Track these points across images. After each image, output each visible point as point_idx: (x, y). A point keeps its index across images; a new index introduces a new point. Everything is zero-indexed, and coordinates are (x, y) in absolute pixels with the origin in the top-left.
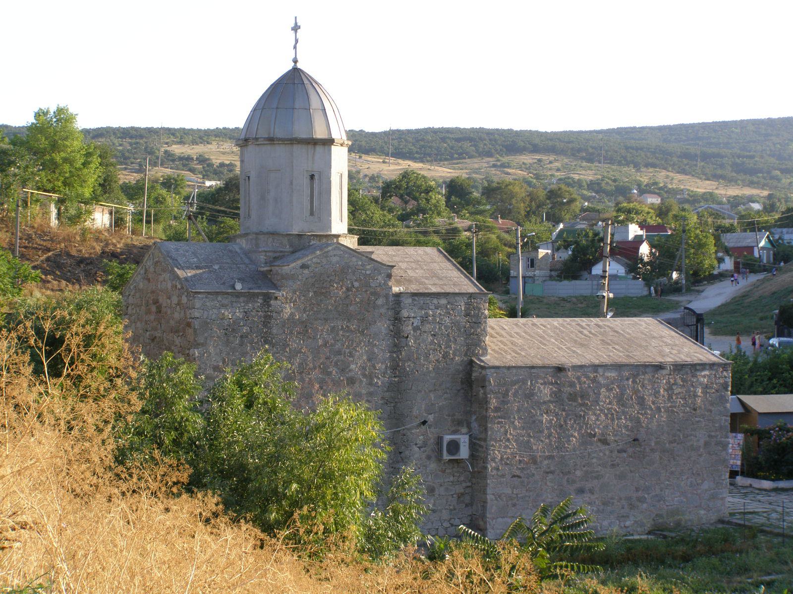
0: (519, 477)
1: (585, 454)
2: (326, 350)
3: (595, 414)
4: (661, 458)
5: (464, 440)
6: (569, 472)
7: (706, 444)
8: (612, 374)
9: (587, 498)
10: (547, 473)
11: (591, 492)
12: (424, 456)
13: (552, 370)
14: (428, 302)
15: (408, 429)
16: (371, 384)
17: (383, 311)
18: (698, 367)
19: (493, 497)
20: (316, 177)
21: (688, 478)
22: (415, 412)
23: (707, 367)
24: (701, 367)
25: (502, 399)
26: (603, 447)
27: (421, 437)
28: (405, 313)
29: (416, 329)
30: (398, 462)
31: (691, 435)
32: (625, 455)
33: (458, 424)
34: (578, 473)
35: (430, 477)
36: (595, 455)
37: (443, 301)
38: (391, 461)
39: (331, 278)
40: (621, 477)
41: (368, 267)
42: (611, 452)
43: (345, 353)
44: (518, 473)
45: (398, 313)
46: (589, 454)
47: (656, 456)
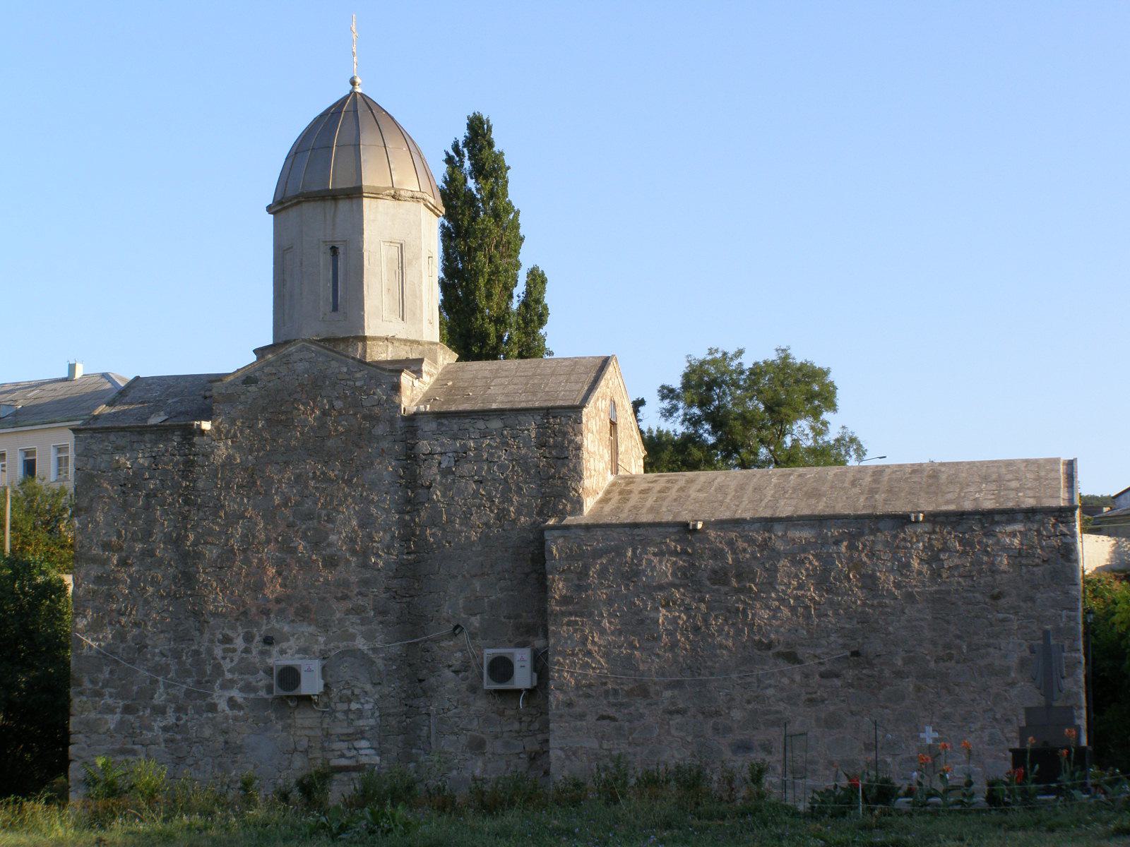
0: (613, 719)
1: (749, 680)
2: (287, 512)
3: (768, 607)
4: (918, 689)
5: (522, 659)
6: (718, 713)
8: (805, 534)
10: (671, 713)
12: (464, 686)
13: (675, 530)
14: (467, 426)
15: (434, 641)
16: (365, 565)
17: (385, 445)
18: (997, 518)
19: (560, 753)
20: (341, 251)
21: (983, 728)
22: (446, 611)
23: (1020, 517)
24: (1004, 518)
25: (577, 582)
26: (784, 666)
27: (459, 655)
28: (424, 446)
29: (446, 472)
30: (416, 697)
31: (988, 646)
32: (837, 682)
34: (737, 714)
35: (475, 722)
36: (772, 682)
37: (496, 424)
38: (403, 695)
39: (296, 396)
40: (832, 722)
41: (358, 375)
42: (807, 676)
43: (319, 516)
44: (611, 712)
45: (413, 447)
46: (759, 680)
47: (909, 685)
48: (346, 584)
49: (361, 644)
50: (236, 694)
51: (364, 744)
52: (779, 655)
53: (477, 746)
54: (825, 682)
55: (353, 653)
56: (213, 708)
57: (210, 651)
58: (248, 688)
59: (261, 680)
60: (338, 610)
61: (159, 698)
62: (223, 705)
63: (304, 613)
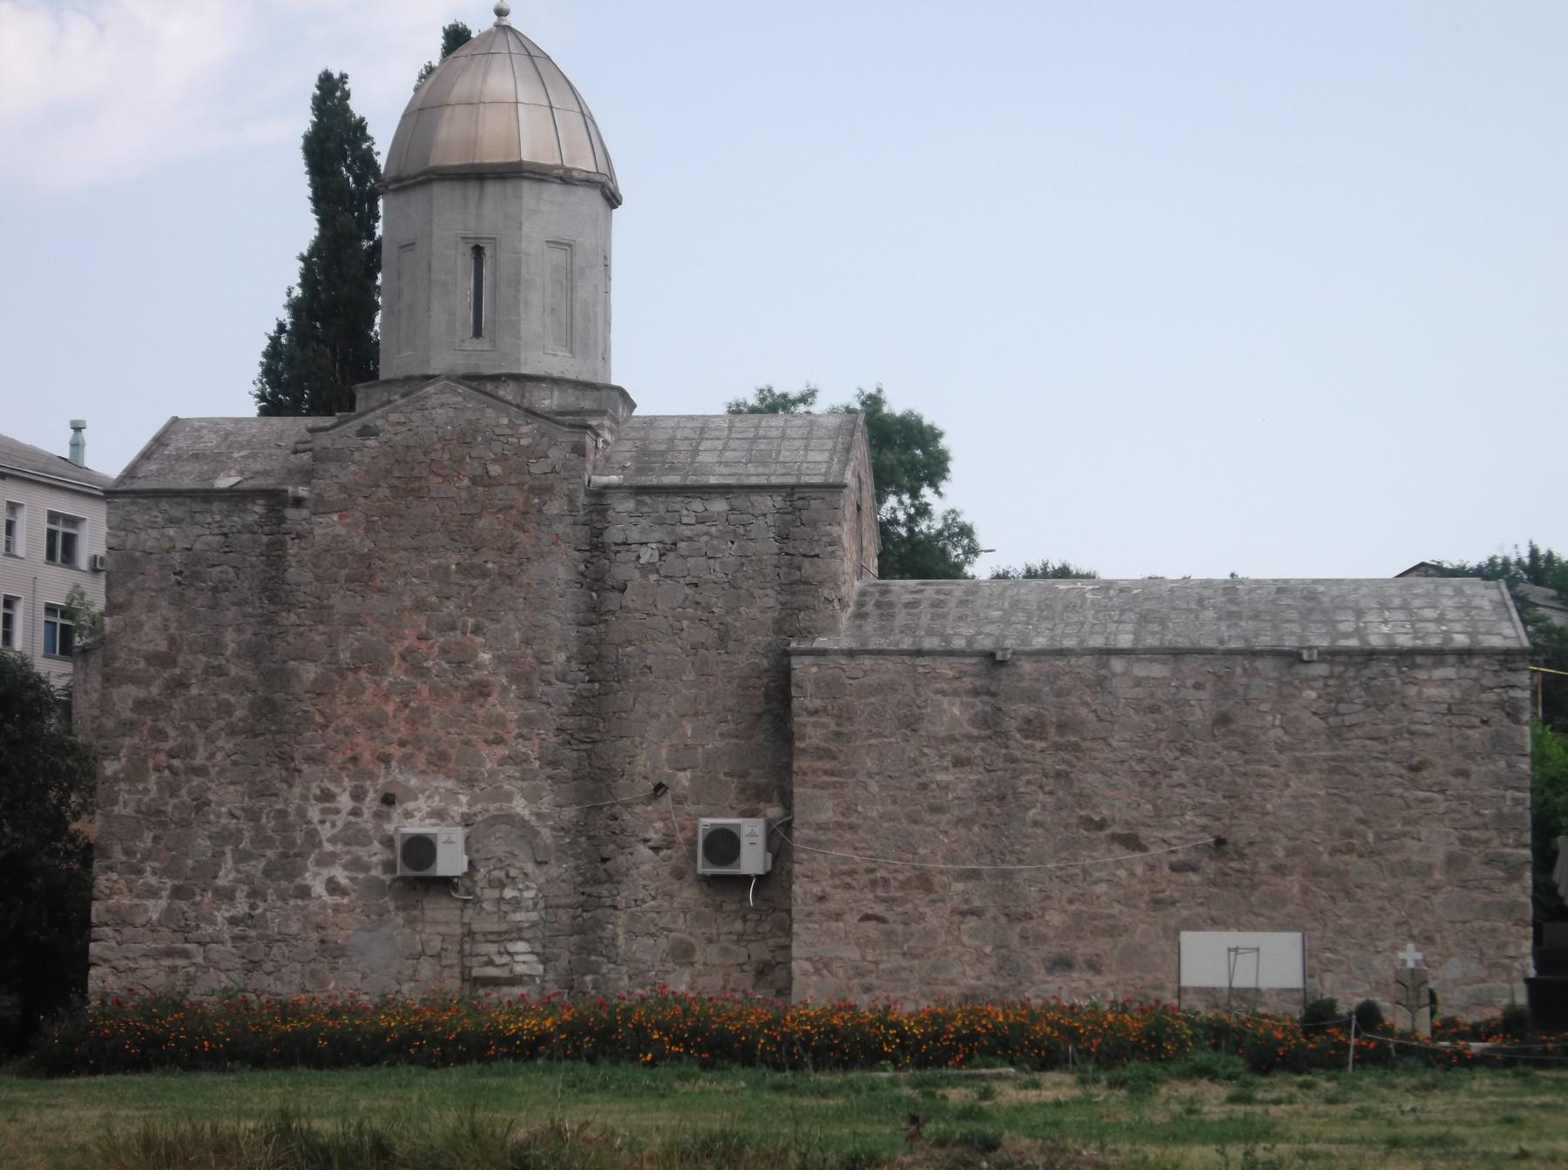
1: (1072, 871)
2: (421, 620)
4: (1305, 891)
6: (1028, 916)
7: (1452, 861)
9: (1082, 984)
10: (963, 914)
11: (1094, 966)
12: (665, 871)
13: (973, 660)
14: (677, 507)
15: (626, 805)
17: (561, 528)
18: (1419, 660)
19: (807, 966)
20: (488, 252)
22: (642, 763)
24: (1428, 661)
25: (833, 727)
27: (659, 825)
28: (614, 534)
29: (649, 568)
30: (597, 882)
31: (1404, 835)
33: (752, 799)
34: (1054, 918)
35: (681, 920)
36: (1104, 875)
37: (718, 506)
38: (579, 879)
39: (433, 456)
41: (525, 429)
42: (1152, 868)
43: (465, 625)
44: (879, 909)
45: (599, 533)
46: (1085, 872)
47: (1292, 884)
48: (500, 722)
49: (520, 806)
50: (342, 876)
51: (520, 946)
52: (1114, 838)
53: (683, 953)
54: (1175, 876)
55: (510, 819)
56: (304, 892)
57: (302, 813)
58: (356, 865)
59: (375, 854)
60: (490, 758)
61: (225, 878)
62: (319, 888)
63: (439, 761)
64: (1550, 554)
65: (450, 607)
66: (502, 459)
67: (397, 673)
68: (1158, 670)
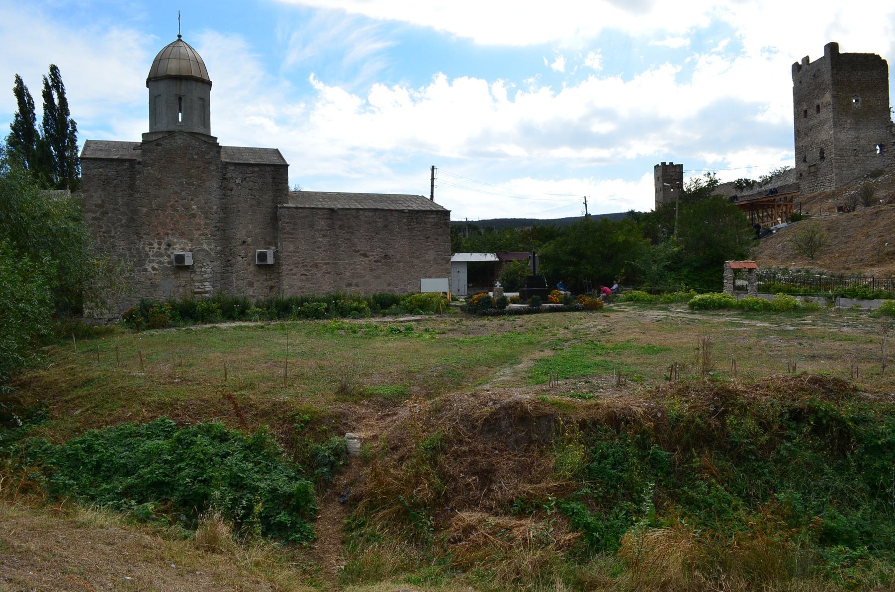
5: (270, 253)
7: (435, 259)
11: (357, 285)
17: (214, 173)
22: (239, 236)
28: (229, 175)
29: (238, 185)
33: (268, 245)
34: (348, 274)
37: (256, 169)
44: (305, 272)
47: (401, 264)
48: (199, 224)
49: (205, 247)
50: (156, 266)
51: (207, 283)
53: (251, 284)
55: (203, 250)
56: (146, 270)
57: (143, 248)
58: (160, 262)
59: (165, 259)
60: (196, 234)
62: (149, 269)
63: (182, 235)
64: (671, 164)
65: (183, 193)
66: (197, 154)
67: (169, 211)
68: (371, 214)
